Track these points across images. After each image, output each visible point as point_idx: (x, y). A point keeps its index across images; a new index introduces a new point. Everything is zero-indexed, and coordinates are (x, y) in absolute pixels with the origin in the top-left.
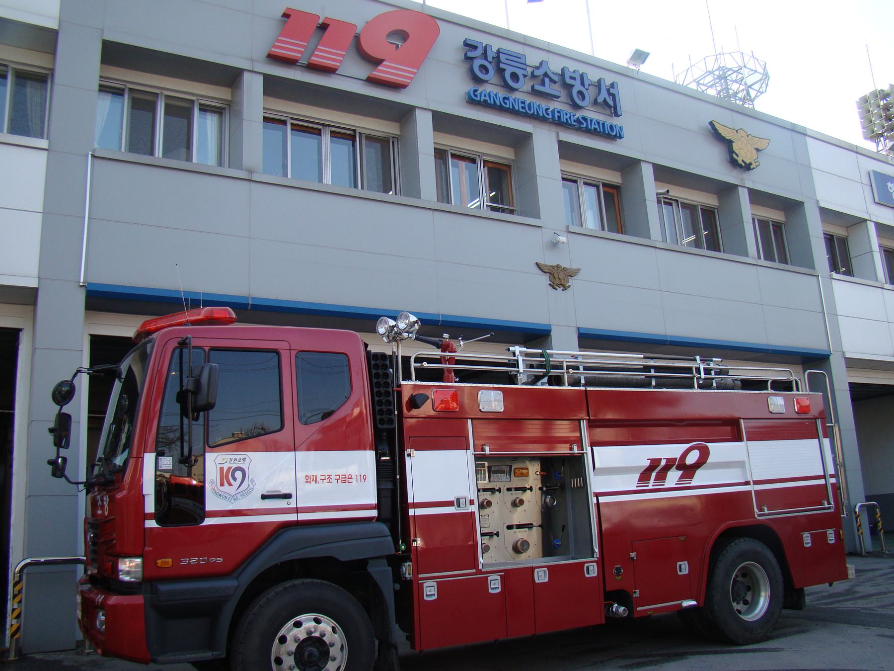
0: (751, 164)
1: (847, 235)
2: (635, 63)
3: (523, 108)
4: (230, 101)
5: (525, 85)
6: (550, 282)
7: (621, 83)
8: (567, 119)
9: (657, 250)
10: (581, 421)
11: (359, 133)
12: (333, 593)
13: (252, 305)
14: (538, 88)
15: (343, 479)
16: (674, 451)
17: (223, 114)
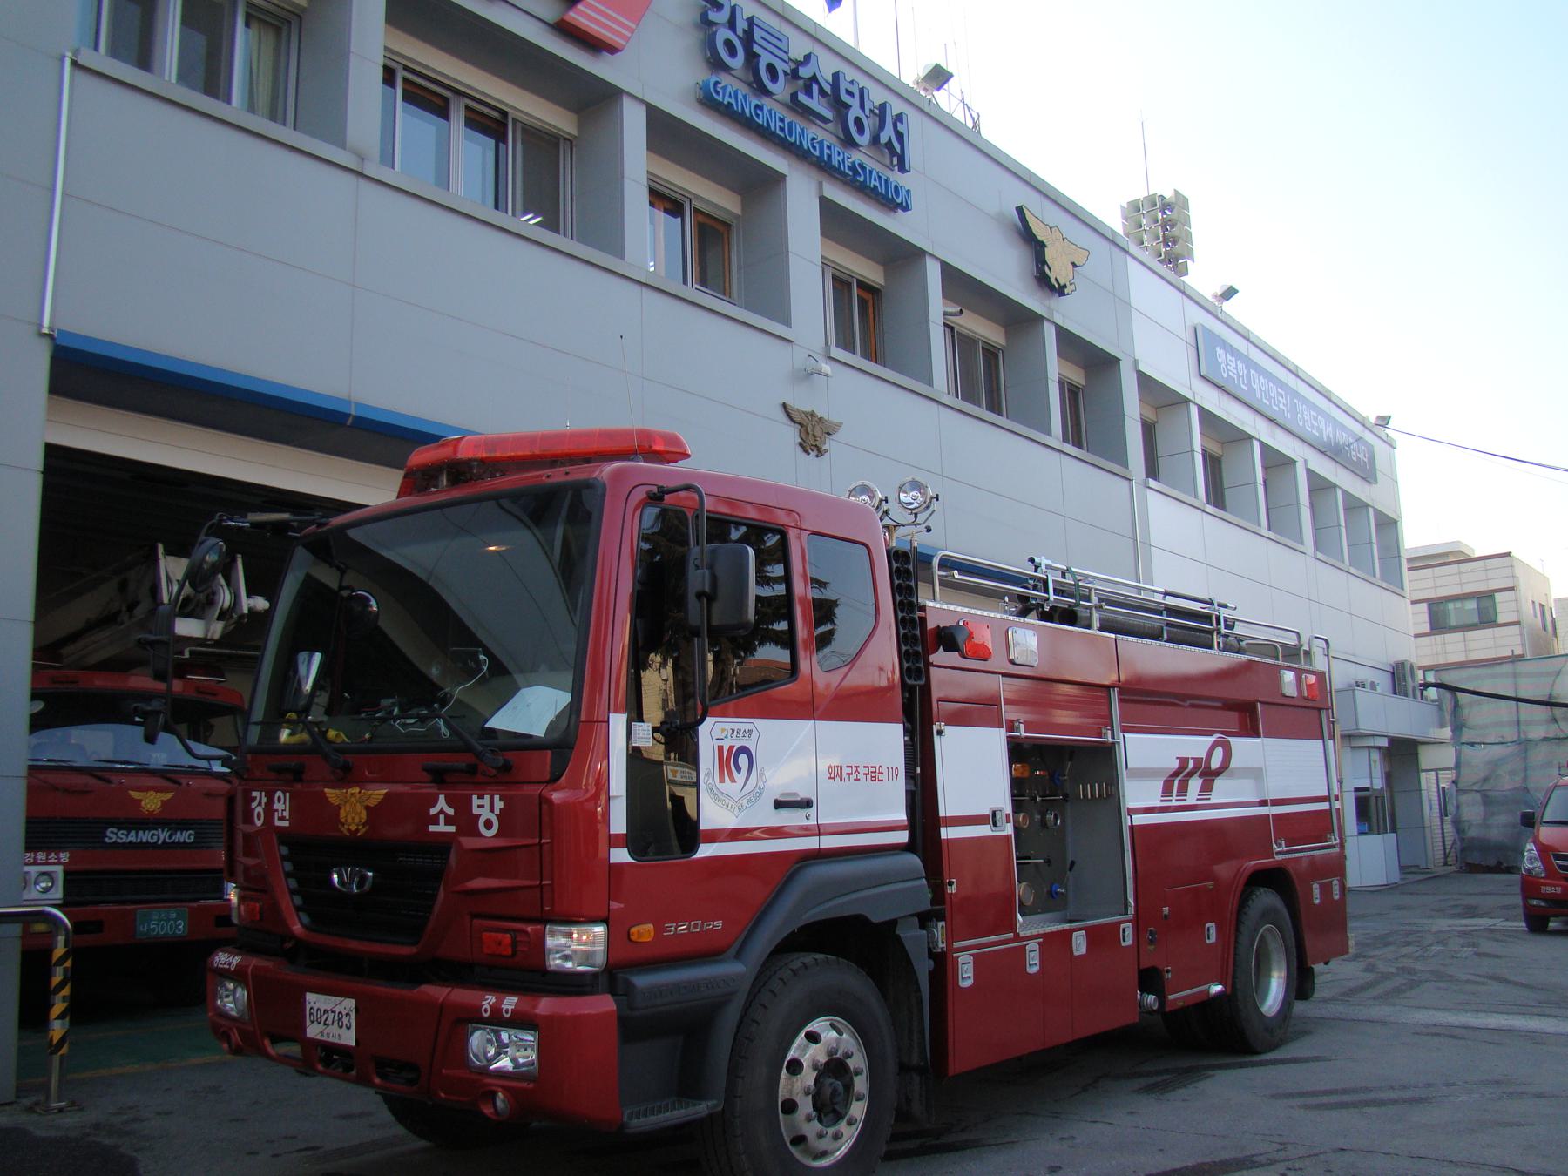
0: (1065, 286)
1: (1156, 420)
2: (928, 86)
3: (782, 129)
4: (304, 9)
5: (780, 89)
6: (800, 440)
7: (912, 117)
8: (839, 161)
9: (941, 408)
10: (1111, 690)
11: (513, 119)
12: (852, 980)
13: (356, 416)
14: (802, 98)
15: (873, 775)
16: (1195, 746)
17: (284, 34)
